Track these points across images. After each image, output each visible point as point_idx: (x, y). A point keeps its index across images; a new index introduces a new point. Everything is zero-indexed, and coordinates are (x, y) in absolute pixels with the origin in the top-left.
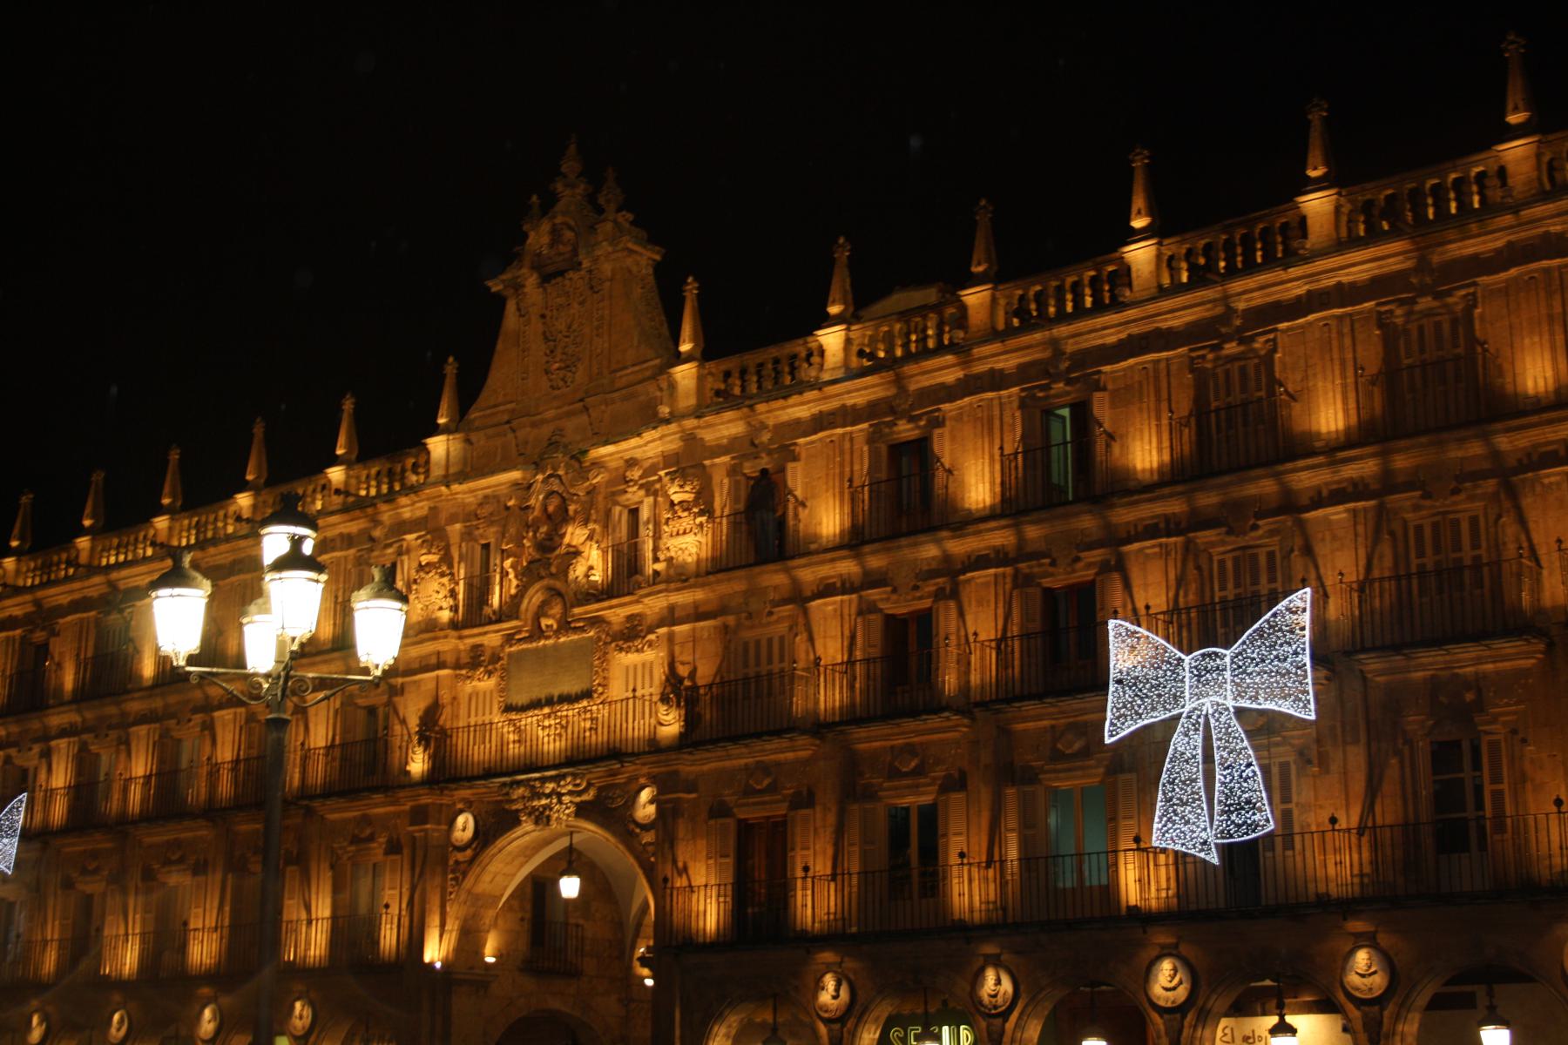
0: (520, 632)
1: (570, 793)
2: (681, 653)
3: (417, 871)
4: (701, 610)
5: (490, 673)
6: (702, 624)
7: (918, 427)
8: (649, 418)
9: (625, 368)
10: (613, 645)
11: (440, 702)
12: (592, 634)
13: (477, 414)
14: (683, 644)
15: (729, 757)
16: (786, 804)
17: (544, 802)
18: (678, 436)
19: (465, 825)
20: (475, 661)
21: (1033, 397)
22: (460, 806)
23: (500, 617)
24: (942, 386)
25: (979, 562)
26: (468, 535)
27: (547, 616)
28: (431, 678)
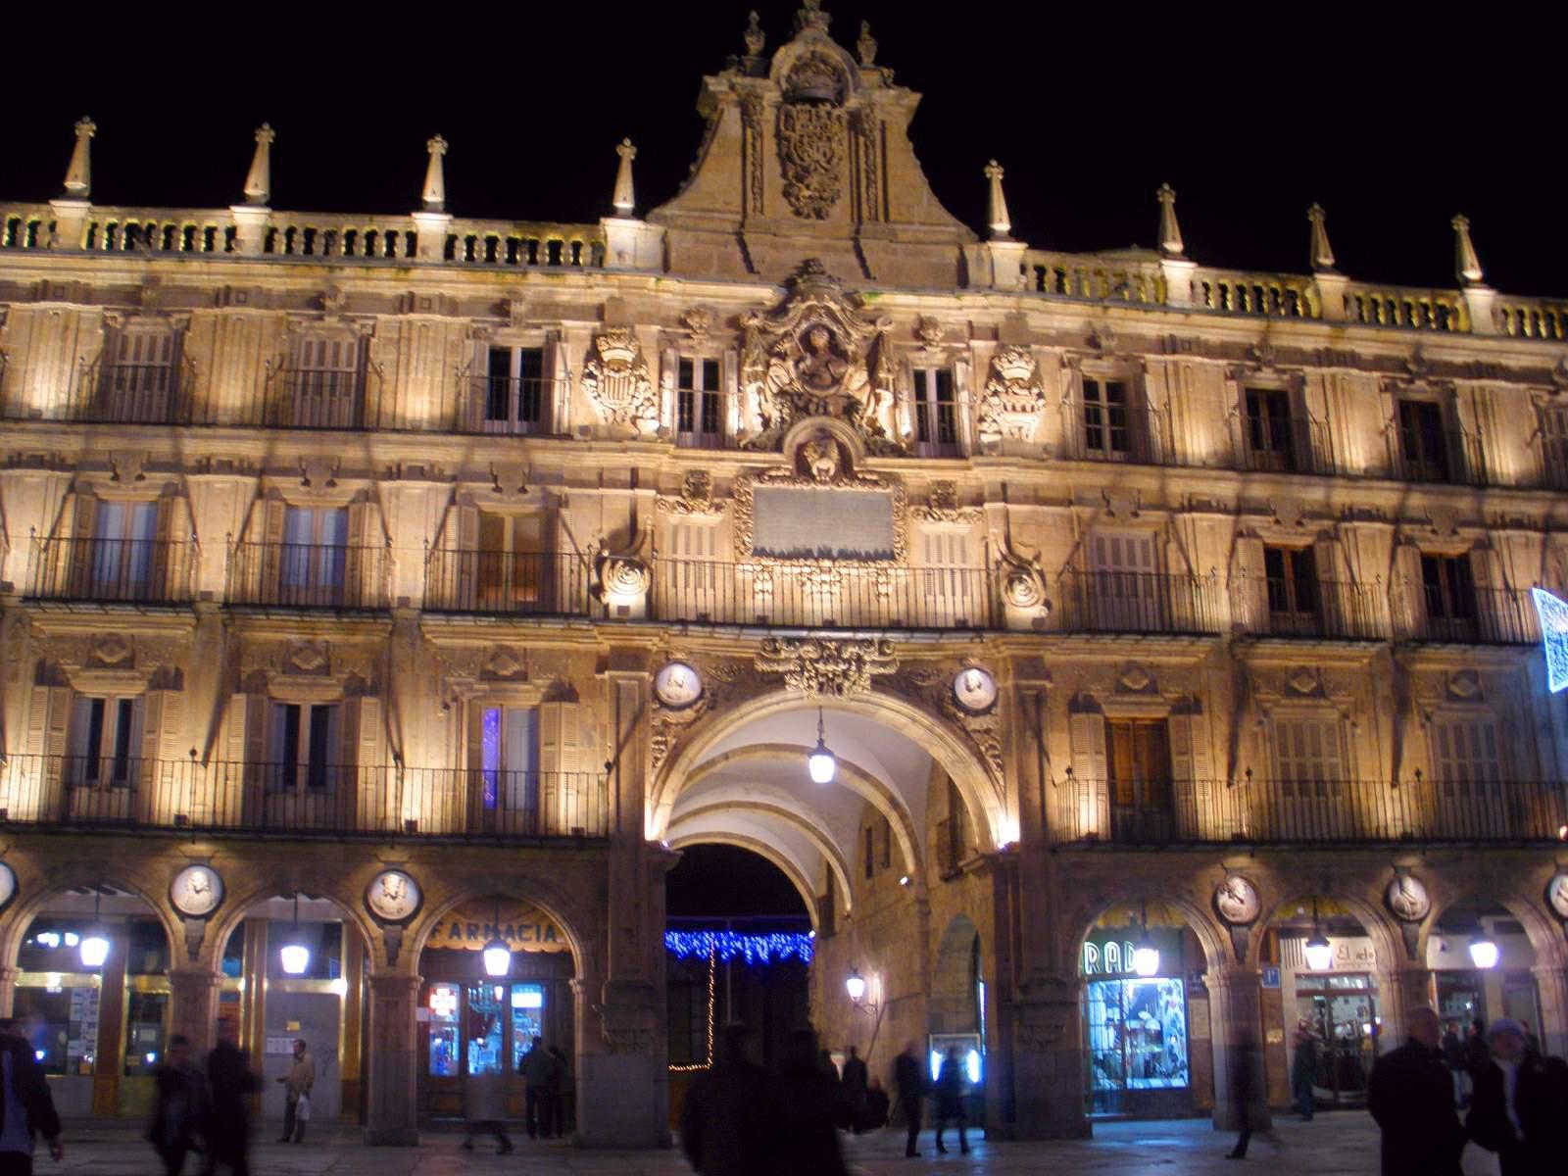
0: (779, 468)
1: (873, 662)
2: (1020, 534)
3: (624, 727)
4: (1041, 494)
5: (718, 508)
6: (1045, 508)
7: (1281, 380)
8: (961, 280)
9: (911, 223)
10: (912, 508)
11: (640, 527)
12: (887, 491)
13: (676, 212)
14: (1022, 526)
15: (1105, 652)
16: (1169, 708)
17: (843, 667)
18: (1006, 311)
19: (681, 682)
20: (697, 488)
21: (1395, 386)
22: (680, 656)
23: (753, 447)
24: (1300, 351)
25: (1368, 515)
26: (668, 340)
27: (823, 455)
28: (624, 497)
